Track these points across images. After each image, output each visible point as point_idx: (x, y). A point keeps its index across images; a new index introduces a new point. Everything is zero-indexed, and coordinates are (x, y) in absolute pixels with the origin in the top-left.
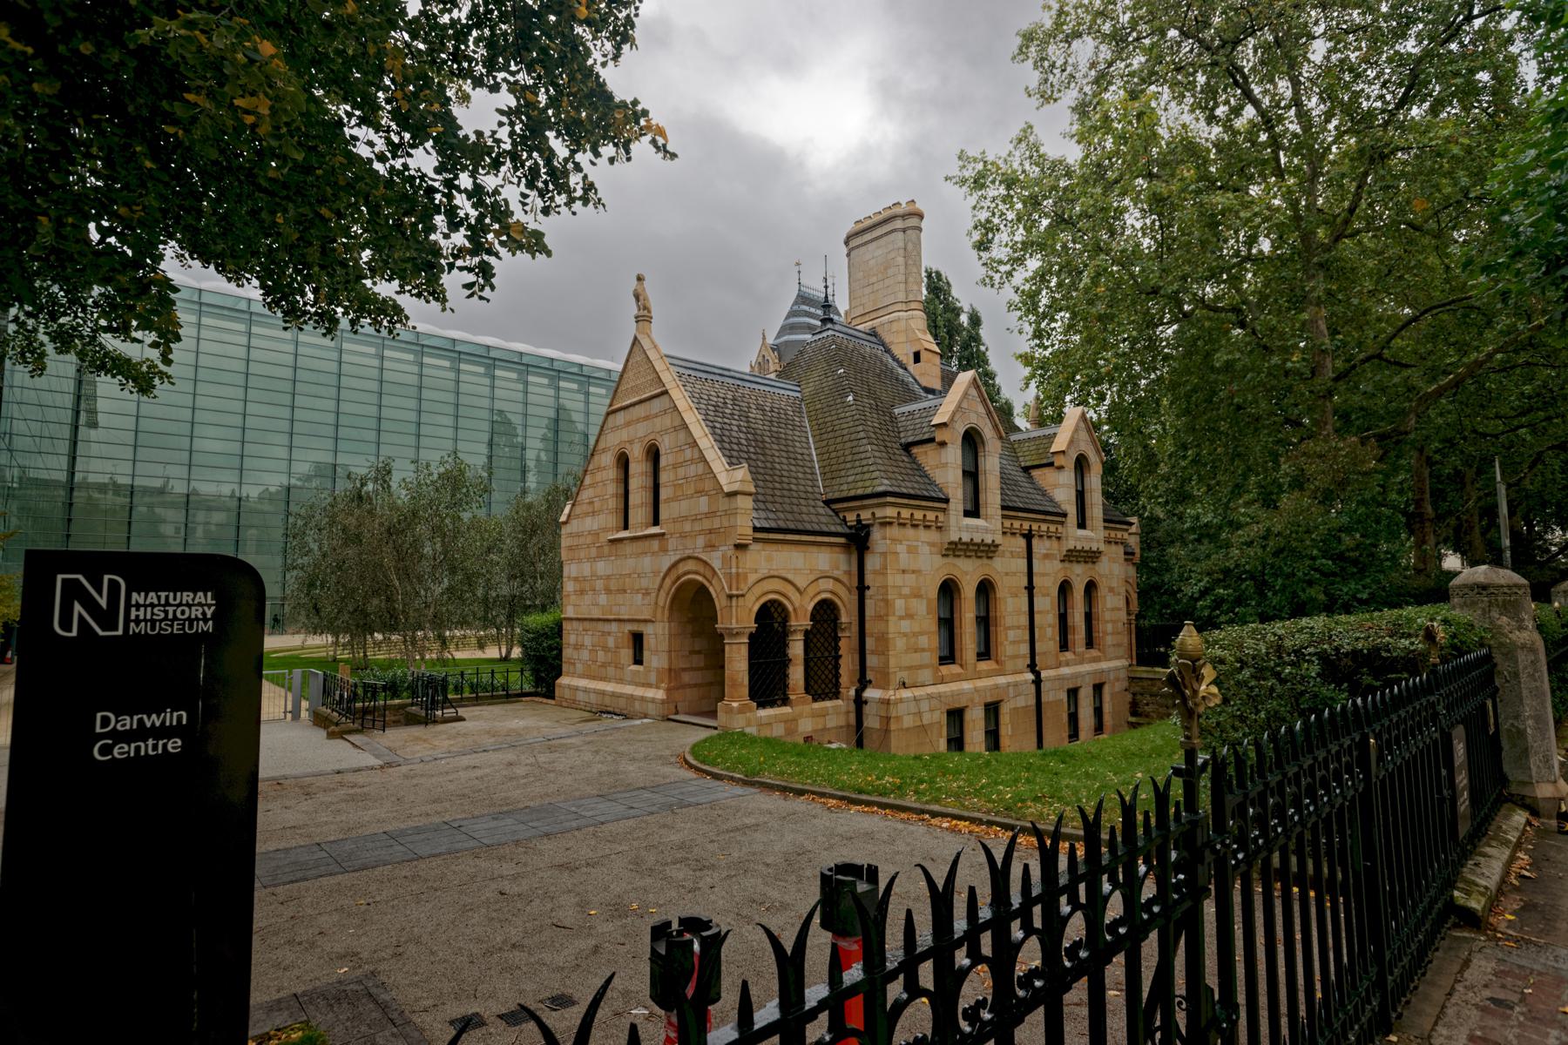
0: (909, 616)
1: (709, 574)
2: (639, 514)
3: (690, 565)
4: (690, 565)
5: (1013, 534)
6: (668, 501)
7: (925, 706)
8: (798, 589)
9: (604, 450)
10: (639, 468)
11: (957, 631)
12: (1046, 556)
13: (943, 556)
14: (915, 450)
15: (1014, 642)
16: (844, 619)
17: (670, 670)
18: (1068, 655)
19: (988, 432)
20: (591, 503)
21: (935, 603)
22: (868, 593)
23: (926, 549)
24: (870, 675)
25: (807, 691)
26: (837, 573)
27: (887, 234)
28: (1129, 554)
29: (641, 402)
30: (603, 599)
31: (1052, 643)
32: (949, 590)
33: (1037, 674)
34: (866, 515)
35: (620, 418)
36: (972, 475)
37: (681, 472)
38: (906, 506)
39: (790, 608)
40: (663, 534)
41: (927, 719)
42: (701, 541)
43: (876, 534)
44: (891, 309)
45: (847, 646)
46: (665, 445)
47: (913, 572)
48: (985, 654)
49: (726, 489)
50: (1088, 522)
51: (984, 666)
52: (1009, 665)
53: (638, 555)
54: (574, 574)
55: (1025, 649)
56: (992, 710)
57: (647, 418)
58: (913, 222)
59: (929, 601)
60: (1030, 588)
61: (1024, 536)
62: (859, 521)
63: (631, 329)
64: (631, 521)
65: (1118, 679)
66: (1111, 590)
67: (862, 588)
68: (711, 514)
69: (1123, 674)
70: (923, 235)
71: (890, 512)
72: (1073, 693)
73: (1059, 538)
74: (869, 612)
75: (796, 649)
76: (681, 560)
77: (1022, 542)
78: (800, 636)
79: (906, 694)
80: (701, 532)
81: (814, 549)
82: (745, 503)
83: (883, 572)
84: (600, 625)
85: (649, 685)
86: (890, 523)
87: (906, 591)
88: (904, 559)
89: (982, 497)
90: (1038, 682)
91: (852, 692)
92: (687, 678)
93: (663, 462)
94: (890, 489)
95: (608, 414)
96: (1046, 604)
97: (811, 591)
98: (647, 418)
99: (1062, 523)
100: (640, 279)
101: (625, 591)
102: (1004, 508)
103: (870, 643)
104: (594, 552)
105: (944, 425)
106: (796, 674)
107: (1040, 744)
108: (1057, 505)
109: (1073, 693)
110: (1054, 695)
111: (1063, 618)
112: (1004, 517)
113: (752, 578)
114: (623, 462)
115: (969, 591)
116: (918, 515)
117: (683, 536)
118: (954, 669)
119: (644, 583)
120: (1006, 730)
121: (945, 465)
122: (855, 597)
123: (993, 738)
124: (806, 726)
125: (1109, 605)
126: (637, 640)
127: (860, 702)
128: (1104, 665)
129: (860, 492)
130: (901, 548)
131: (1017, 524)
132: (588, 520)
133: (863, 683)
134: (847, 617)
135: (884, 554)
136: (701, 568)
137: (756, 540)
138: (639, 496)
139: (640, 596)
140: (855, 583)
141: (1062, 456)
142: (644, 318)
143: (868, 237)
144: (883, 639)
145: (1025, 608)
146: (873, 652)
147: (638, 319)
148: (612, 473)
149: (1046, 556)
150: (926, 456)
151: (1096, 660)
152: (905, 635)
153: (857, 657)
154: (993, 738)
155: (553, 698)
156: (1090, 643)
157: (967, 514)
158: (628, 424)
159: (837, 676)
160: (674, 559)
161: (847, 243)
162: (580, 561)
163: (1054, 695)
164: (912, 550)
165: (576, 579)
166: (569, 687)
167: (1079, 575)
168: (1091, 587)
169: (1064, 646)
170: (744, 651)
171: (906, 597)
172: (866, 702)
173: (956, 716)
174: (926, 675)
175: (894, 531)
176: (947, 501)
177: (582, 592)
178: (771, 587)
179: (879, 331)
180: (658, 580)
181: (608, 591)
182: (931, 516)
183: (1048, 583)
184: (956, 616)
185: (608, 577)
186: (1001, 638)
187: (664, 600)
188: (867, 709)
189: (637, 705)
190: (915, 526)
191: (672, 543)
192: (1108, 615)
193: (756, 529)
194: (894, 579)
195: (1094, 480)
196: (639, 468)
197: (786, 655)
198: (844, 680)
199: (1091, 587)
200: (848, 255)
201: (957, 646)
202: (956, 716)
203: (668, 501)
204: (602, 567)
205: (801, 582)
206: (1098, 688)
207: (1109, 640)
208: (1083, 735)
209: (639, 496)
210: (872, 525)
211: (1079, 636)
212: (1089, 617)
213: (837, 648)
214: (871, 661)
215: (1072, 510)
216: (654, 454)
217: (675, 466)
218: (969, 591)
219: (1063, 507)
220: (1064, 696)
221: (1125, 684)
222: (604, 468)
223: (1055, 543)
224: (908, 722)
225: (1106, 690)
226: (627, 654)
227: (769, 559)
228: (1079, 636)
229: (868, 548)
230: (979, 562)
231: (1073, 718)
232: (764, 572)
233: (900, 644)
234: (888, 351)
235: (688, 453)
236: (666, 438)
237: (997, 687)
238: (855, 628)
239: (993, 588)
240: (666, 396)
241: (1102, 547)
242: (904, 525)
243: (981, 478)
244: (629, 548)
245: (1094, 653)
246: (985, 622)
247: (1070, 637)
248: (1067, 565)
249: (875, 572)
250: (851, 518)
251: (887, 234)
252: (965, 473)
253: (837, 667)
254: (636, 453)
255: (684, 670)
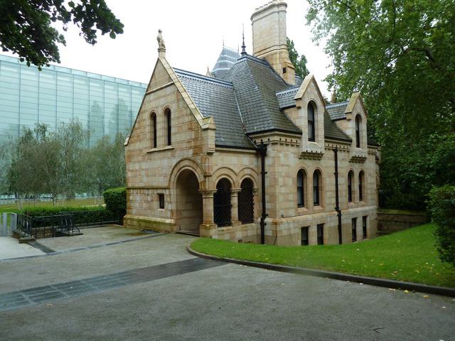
0: (285, 185)
1: (195, 166)
2: (161, 140)
3: (186, 163)
4: (186, 163)
5: (329, 149)
6: (175, 134)
7: (292, 225)
8: (235, 174)
9: (144, 112)
10: (161, 120)
11: (305, 192)
12: (343, 159)
13: (300, 159)
14: (286, 111)
15: (329, 198)
16: (255, 187)
17: (177, 210)
18: (352, 204)
19: (319, 103)
20: (139, 136)
21: (296, 180)
22: (266, 175)
23: (292, 155)
24: (267, 212)
25: (240, 219)
26: (252, 166)
27: (271, 14)
28: (377, 159)
29: (162, 88)
30: (145, 179)
31: (345, 198)
32: (302, 174)
33: (339, 212)
34: (265, 140)
35: (152, 96)
36: (312, 123)
37: (181, 120)
38: (284, 136)
39: (232, 182)
40: (173, 149)
41: (292, 231)
42: (191, 152)
43: (270, 149)
44: (272, 49)
45: (257, 200)
46: (173, 108)
47: (287, 166)
48: (317, 203)
49: (203, 127)
50: (361, 145)
51: (317, 208)
52: (327, 208)
53: (161, 159)
54: (131, 169)
55: (334, 201)
56: (320, 228)
57: (165, 96)
58: (282, 8)
59: (293, 179)
60: (336, 174)
61: (333, 150)
62: (262, 143)
63: (156, 55)
64: (157, 144)
65: (373, 214)
66: (370, 175)
67: (263, 173)
68: (196, 139)
69: (375, 212)
70: (287, 15)
71: (277, 138)
72: (354, 220)
73: (348, 152)
74: (267, 183)
75: (235, 201)
76: (181, 161)
77: (333, 153)
78: (236, 195)
79: (283, 220)
80: (191, 148)
81: (242, 155)
82: (211, 134)
83: (273, 165)
84: (146, 192)
85: (168, 218)
86: (277, 143)
87: (283, 174)
88: (283, 160)
89: (316, 132)
90: (339, 216)
91: (259, 220)
92: (185, 214)
93: (172, 116)
94: (277, 128)
95: (146, 95)
96: (343, 181)
97: (241, 174)
98: (165, 96)
99: (350, 145)
100: (160, 32)
101: (155, 175)
102: (325, 137)
103: (267, 198)
104: (140, 158)
105: (300, 99)
106: (235, 212)
107: (340, 242)
108: (347, 136)
109: (354, 220)
110: (346, 221)
111: (350, 187)
112: (326, 141)
113: (215, 168)
114: (153, 116)
115: (310, 174)
116: (289, 140)
117: (182, 149)
118: (304, 209)
119: (164, 171)
120: (326, 236)
121: (300, 117)
122: (260, 177)
123: (321, 240)
124: (239, 235)
125: (369, 182)
126: (161, 197)
127: (263, 224)
128: (367, 208)
129: (263, 129)
130: (281, 155)
131: (331, 145)
132: (138, 143)
133: (264, 215)
134: (257, 186)
135: (273, 158)
136: (191, 164)
137: (216, 151)
138: (161, 132)
139: (162, 177)
140: (260, 171)
141: (349, 115)
142: (162, 49)
143: (261, 16)
144: (274, 196)
145: (334, 182)
146: (268, 202)
147: (159, 50)
148: (148, 122)
149: (343, 159)
150: (291, 114)
151: (363, 206)
152: (283, 194)
153: (261, 204)
154: (321, 240)
155: (122, 225)
156: (361, 198)
157: (310, 140)
158: (155, 99)
159: (252, 212)
160: (178, 160)
161: (252, 19)
162: (134, 163)
163: (346, 221)
164: (286, 156)
165: (132, 171)
166: (130, 219)
167: (357, 168)
168: (362, 174)
169: (350, 200)
170: (212, 201)
171: (283, 177)
172: (266, 224)
173: (305, 230)
174: (292, 212)
175: (278, 147)
176: (301, 134)
177: (135, 176)
178: (222, 173)
179: (267, 59)
180: (171, 170)
181: (147, 176)
182: (294, 140)
183: (343, 172)
184: (305, 186)
185: (147, 170)
186: (324, 195)
187: (174, 179)
188: (266, 227)
189: (162, 227)
190: (287, 145)
191: (177, 153)
192: (369, 186)
193: (217, 146)
194: (278, 169)
195: (363, 126)
196: (161, 120)
197: (230, 203)
198: (255, 214)
199: (362, 174)
200: (252, 24)
201: (305, 199)
202: (305, 230)
203: (175, 134)
204: (144, 165)
205: (237, 171)
206: (365, 218)
207: (369, 197)
208: (358, 238)
209: (161, 132)
210: (268, 144)
211: (356, 195)
212: (360, 187)
213: (252, 200)
214: (268, 205)
215: (354, 139)
216: (168, 113)
217: (178, 118)
218: (310, 174)
219: (350, 137)
220: (350, 222)
221: (376, 216)
222: (144, 120)
223: (347, 154)
224: (285, 233)
225: (368, 219)
226: (156, 204)
227: (222, 160)
228: (356, 195)
229: (266, 155)
230: (315, 161)
231: (354, 231)
232: (220, 166)
233: (280, 198)
234: (271, 68)
235: (184, 112)
236: (174, 105)
237: (322, 217)
238: (260, 191)
239: (320, 173)
240: (173, 86)
241: (367, 156)
242: (282, 144)
243: (316, 124)
244: (157, 156)
245: (362, 202)
246: (317, 189)
247: (352, 196)
248: (351, 163)
249: (270, 166)
250: (258, 141)
251: (271, 14)
252: (309, 121)
253: (252, 208)
254: (160, 113)
255: (183, 210)
